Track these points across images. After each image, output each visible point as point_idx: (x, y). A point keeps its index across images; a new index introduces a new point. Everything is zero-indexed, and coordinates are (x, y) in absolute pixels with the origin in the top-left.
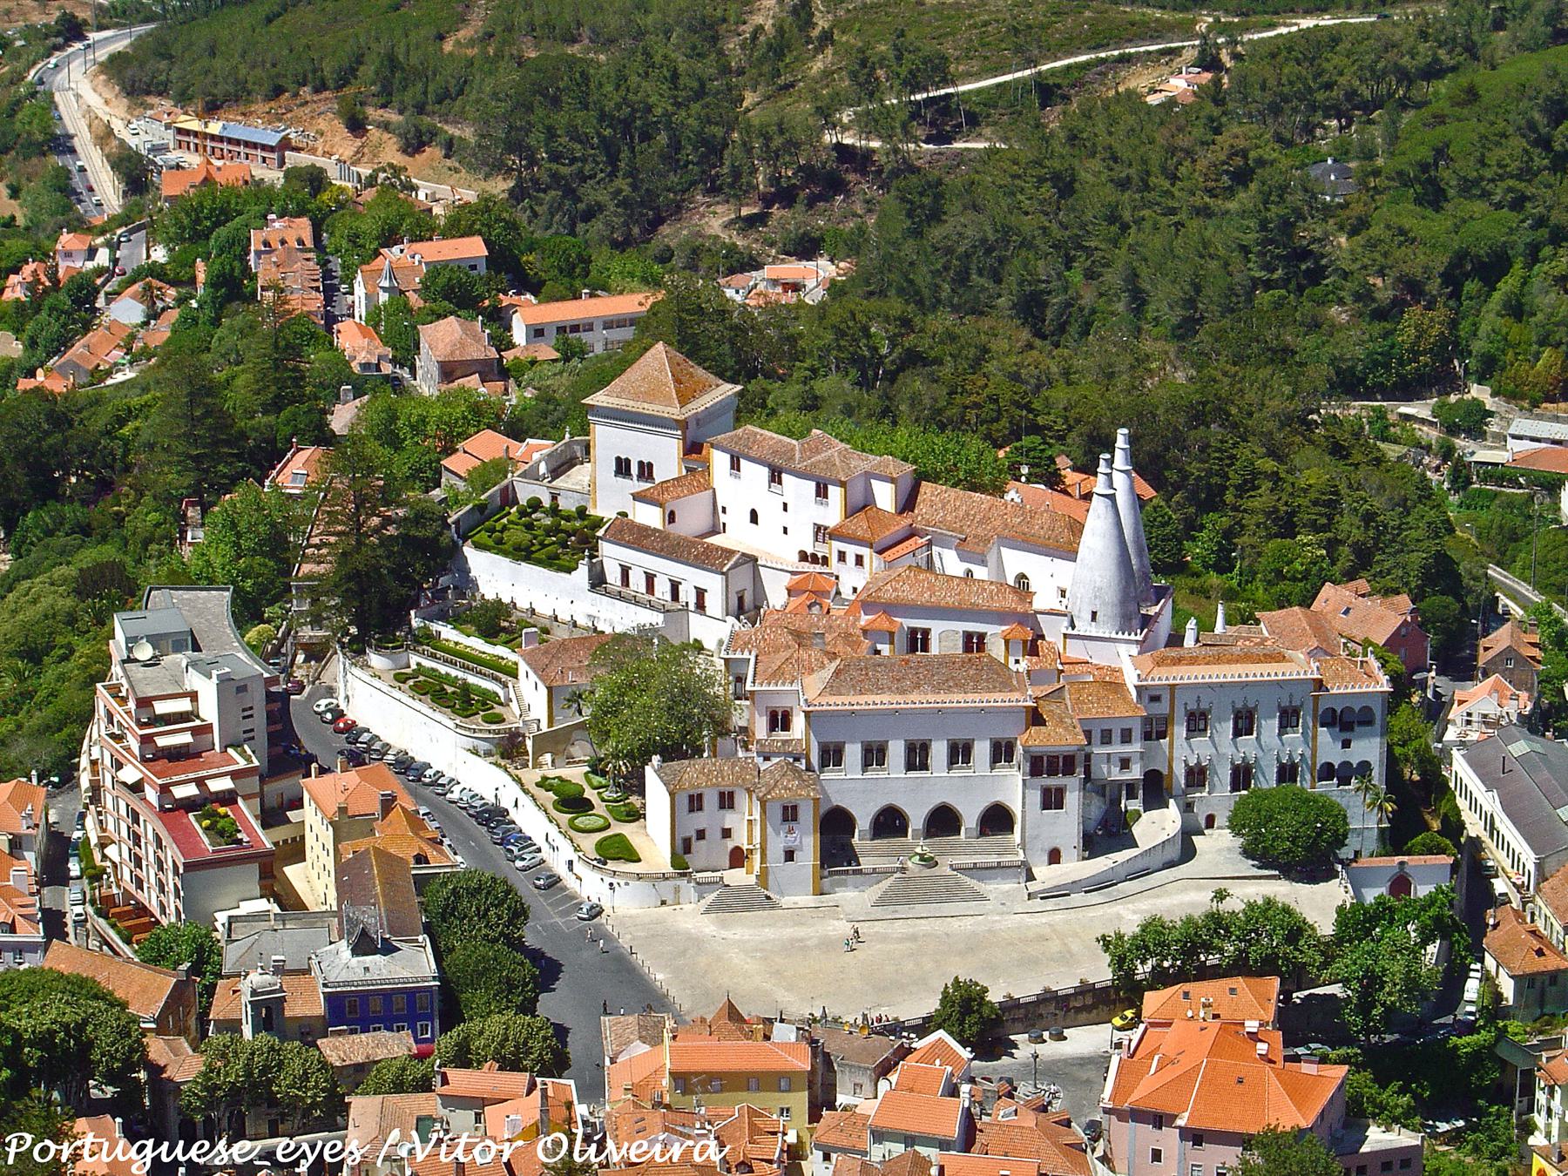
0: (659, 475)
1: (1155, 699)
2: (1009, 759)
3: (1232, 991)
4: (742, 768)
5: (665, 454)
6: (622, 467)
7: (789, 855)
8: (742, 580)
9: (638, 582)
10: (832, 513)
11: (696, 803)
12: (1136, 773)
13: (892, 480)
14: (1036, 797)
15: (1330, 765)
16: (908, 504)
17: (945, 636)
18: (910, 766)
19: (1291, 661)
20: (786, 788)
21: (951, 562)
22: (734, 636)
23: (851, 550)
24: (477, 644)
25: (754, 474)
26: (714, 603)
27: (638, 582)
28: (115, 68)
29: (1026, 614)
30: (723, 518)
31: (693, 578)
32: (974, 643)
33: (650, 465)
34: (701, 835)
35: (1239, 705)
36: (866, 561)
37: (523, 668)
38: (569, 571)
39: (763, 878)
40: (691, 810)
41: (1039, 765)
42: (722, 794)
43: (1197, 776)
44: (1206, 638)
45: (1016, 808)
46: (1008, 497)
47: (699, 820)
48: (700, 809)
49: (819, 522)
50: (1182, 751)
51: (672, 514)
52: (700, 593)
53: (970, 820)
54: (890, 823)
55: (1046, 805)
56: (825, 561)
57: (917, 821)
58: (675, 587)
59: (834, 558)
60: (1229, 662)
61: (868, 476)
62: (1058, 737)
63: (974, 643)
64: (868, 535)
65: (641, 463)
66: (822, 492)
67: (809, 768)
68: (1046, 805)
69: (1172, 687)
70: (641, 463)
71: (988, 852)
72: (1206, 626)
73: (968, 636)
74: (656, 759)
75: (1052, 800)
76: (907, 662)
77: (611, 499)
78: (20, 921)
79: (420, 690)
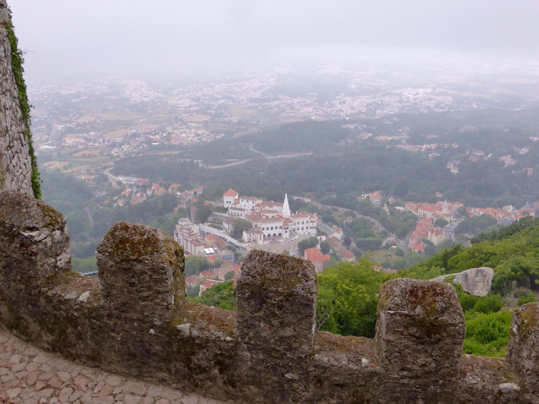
6: (227, 202)
9: (233, 214)
27: (233, 214)
28: (111, 172)
31: (240, 212)
32: (273, 217)
37: (224, 223)
43: (298, 229)
50: (297, 226)
53: (277, 235)
57: (272, 235)
66: (253, 202)
72: (295, 213)
75: (286, 232)
77: (226, 205)
79: (212, 227)
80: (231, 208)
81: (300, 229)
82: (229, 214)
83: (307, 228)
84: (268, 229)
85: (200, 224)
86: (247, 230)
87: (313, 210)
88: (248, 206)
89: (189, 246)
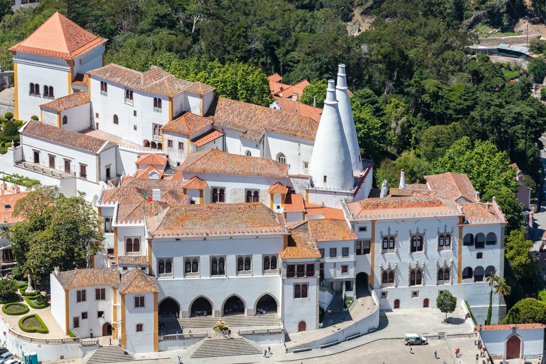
0: (57, 94)
1: (363, 229)
2: (274, 266)
4: (110, 274)
5: (60, 81)
6: (34, 89)
7: (139, 328)
10: (164, 117)
12: (351, 274)
13: (201, 97)
14: (290, 290)
15: (469, 269)
16: (210, 111)
18: (213, 272)
19: (445, 205)
20: (137, 286)
21: (235, 146)
22: (104, 193)
23: (176, 140)
25: (116, 93)
29: (284, 178)
30: (96, 120)
31: (78, 157)
33: (51, 88)
34: (85, 315)
35: (414, 232)
36: (185, 146)
39: (123, 341)
40: (79, 300)
41: (292, 271)
42: (97, 290)
43: (389, 277)
44: (393, 191)
46: (272, 106)
47: (84, 306)
48: (84, 299)
49: (157, 122)
52: (83, 168)
53: (250, 303)
54: (201, 306)
55: (297, 295)
56: (160, 146)
57: (218, 305)
58: (67, 163)
59: (165, 145)
60: (408, 206)
61: (186, 93)
63: (252, 196)
64: (186, 130)
65: (46, 87)
66: (157, 103)
67: (151, 274)
68: (297, 295)
69: (373, 222)
70: (46, 87)
75: (301, 292)
76: (211, 208)
77: (27, 108)
82: (20, 162)
84: (191, 266)
88: (128, 116)
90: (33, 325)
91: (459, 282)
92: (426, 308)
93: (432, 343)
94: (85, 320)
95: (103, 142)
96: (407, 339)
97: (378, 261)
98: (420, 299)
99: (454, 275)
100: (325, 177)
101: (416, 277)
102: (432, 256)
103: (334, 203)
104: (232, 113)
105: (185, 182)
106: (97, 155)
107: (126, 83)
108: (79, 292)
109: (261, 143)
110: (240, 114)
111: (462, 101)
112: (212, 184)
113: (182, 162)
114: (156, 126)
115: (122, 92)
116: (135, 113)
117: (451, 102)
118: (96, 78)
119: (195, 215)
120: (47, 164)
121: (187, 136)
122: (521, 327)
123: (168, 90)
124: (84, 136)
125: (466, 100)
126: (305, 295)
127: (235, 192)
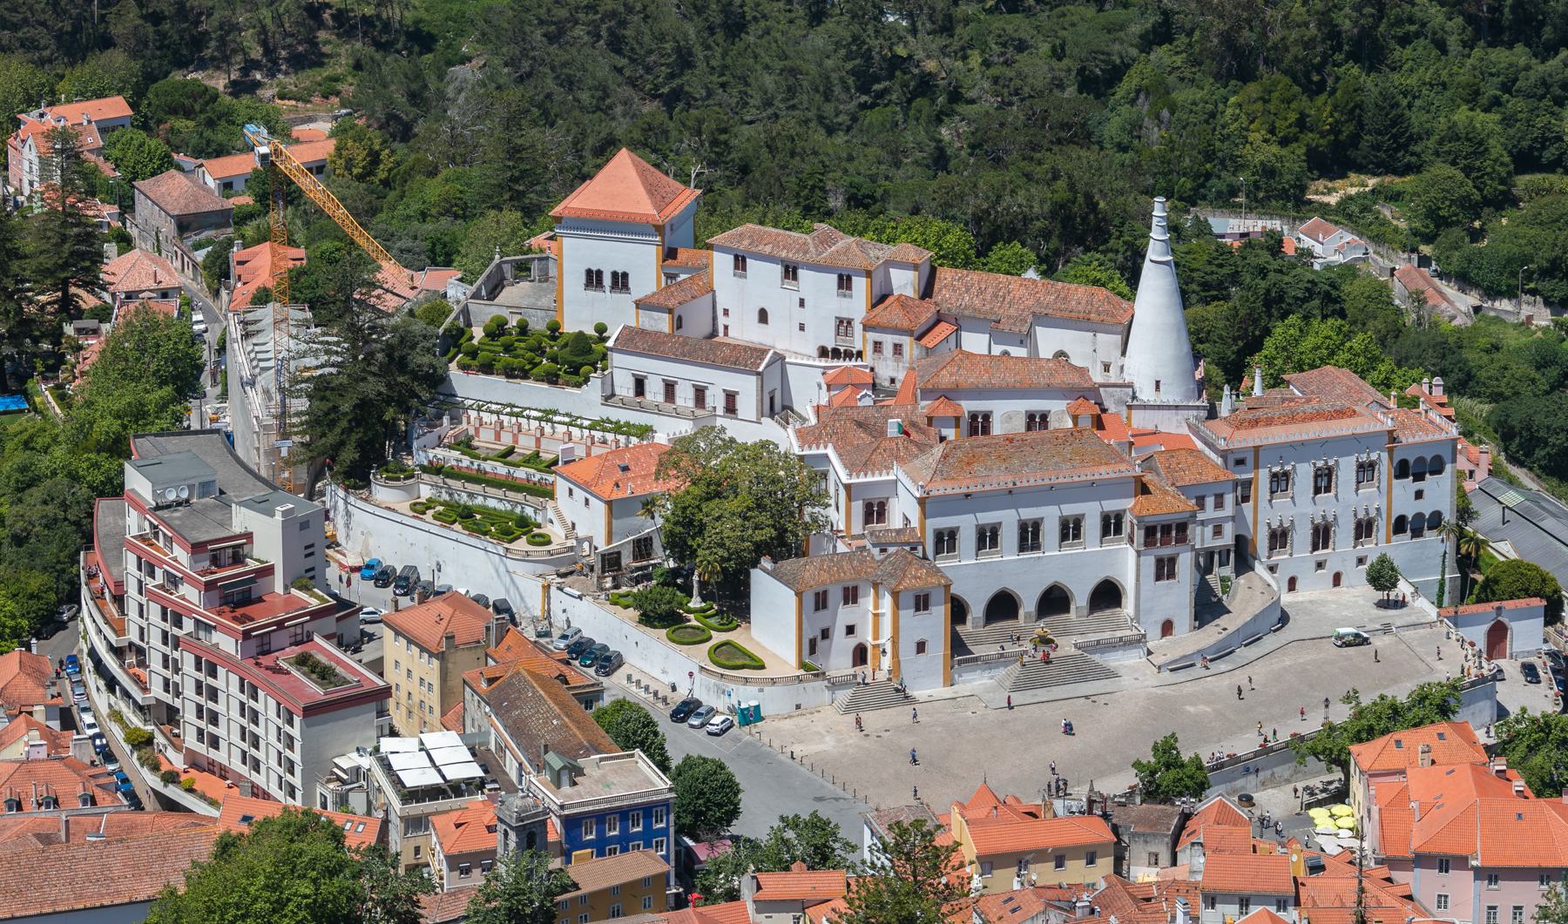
1: (1240, 462)
2: (1118, 531)
3: (1441, 736)
5: (640, 261)
6: (593, 279)
7: (921, 647)
8: (774, 383)
10: (857, 304)
11: (821, 602)
12: (1228, 539)
13: (915, 267)
16: (927, 292)
17: (1007, 415)
19: (1361, 415)
23: (888, 340)
24: (502, 470)
25: (764, 274)
26: (748, 404)
29: (1089, 389)
30: (722, 320)
31: (719, 382)
32: (1037, 421)
33: (625, 275)
34: (825, 634)
36: (906, 350)
37: (562, 487)
38: (578, 385)
39: (896, 669)
41: (1155, 533)
42: (846, 590)
43: (1279, 538)
44: (1243, 404)
45: (1128, 584)
47: (823, 619)
48: (825, 607)
49: (844, 315)
51: (680, 318)
52: (731, 398)
57: (1028, 605)
60: (1304, 420)
61: (890, 263)
62: (1167, 504)
63: (1037, 421)
64: (906, 324)
65: (615, 274)
66: (845, 282)
67: (925, 558)
69: (1257, 449)
70: (615, 274)
71: (1103, 627)
73: (1031, 417)
74: (766, 562)
77: (581, 313)
78: (99, 793)
80: (635, 341)
81: (1302, 537)
82: (609, 397)
83: (1364, 529)
84: (987, 538)
85: (334, 495)
86: (783, 544)
87: (1397, 349)
89: (228, 707)
90: (735, 660)
91: (1388, 541)
92: (1337, 589)
93: (1379, 642)
94: (826, 642)
95: (764, 352)
96: (1340, 637)
97: (1266, 512)
98: (1327, 573)
99: (1382, 528)
100: (1158, 383)
101: (1322, 535)
102: (1349, 499)
103: (1173, 424)
104: (967, 291)
105: (925, 406)
106: (758, 374)
107: (784, 254)
108: (817, 594)
109: (1026, 339)
110: (981, 292)
111: (1214, 268)
112: (968, 406)
113: (900, 376)
114: (841, 322)
115: (778, 269)
116: (802, 303)
117: (1192, 270)
118: (723, 249)
119: (988, 454)
120: (661, 398)
121: (909, 333)
122: (1509, 605)
123: (859, 261)
124: (711, 348)
125: (1221, 266)
126: (1171, 575)
127: (1009, 417)
